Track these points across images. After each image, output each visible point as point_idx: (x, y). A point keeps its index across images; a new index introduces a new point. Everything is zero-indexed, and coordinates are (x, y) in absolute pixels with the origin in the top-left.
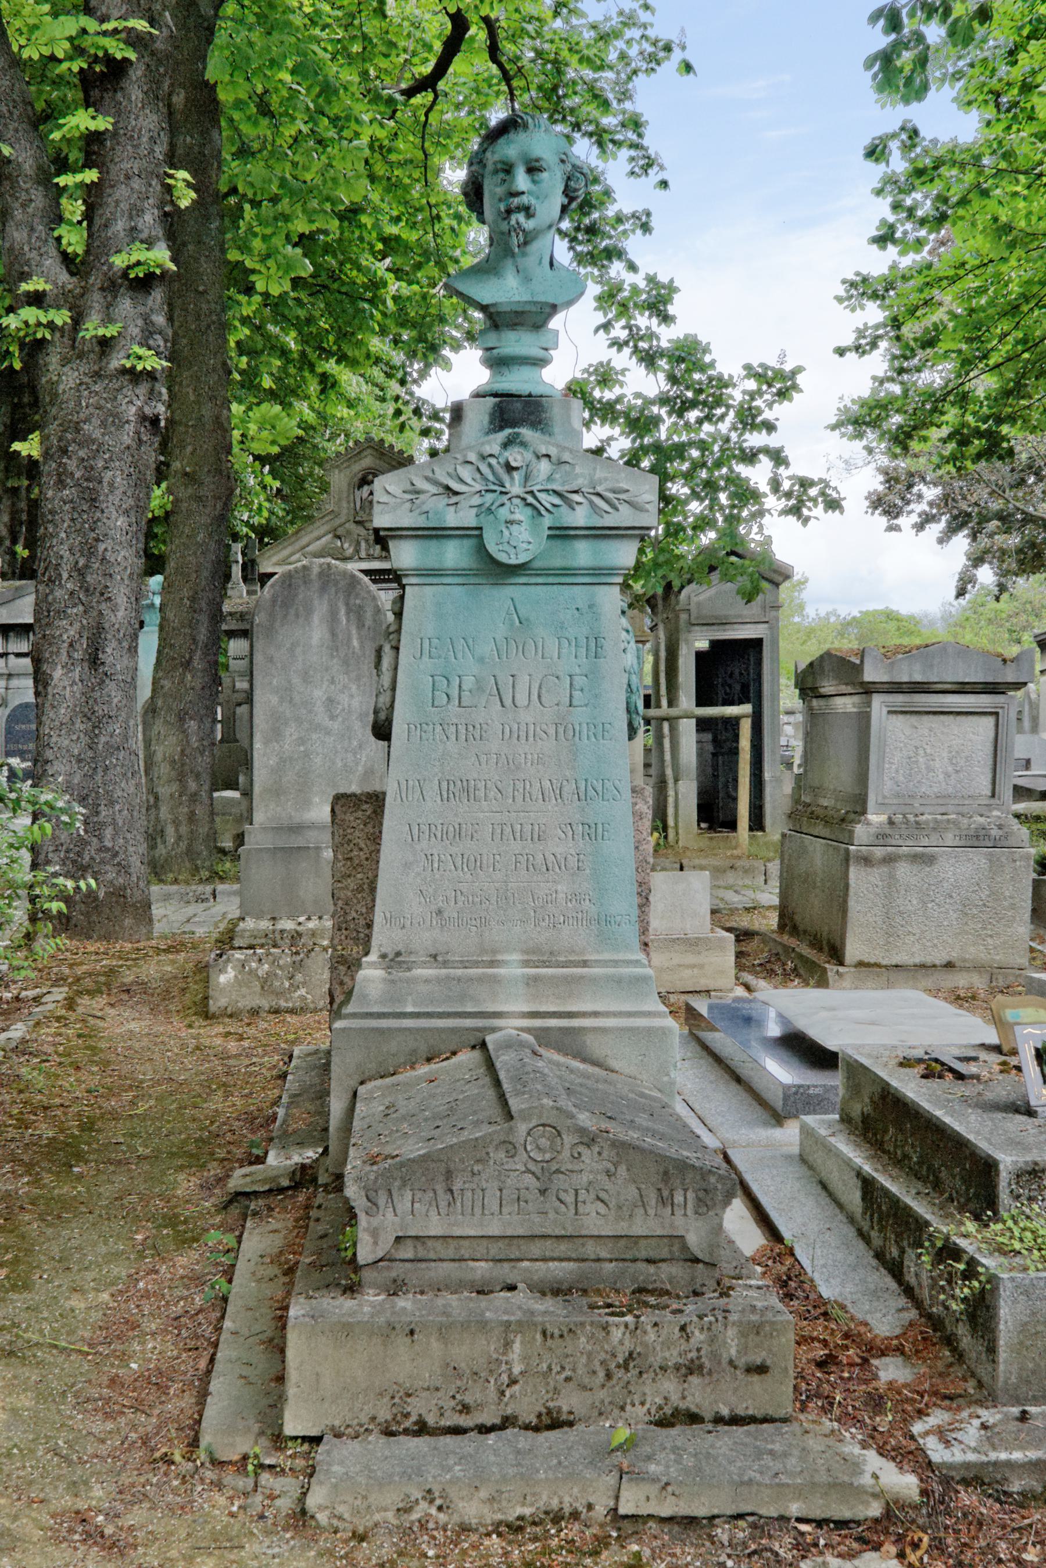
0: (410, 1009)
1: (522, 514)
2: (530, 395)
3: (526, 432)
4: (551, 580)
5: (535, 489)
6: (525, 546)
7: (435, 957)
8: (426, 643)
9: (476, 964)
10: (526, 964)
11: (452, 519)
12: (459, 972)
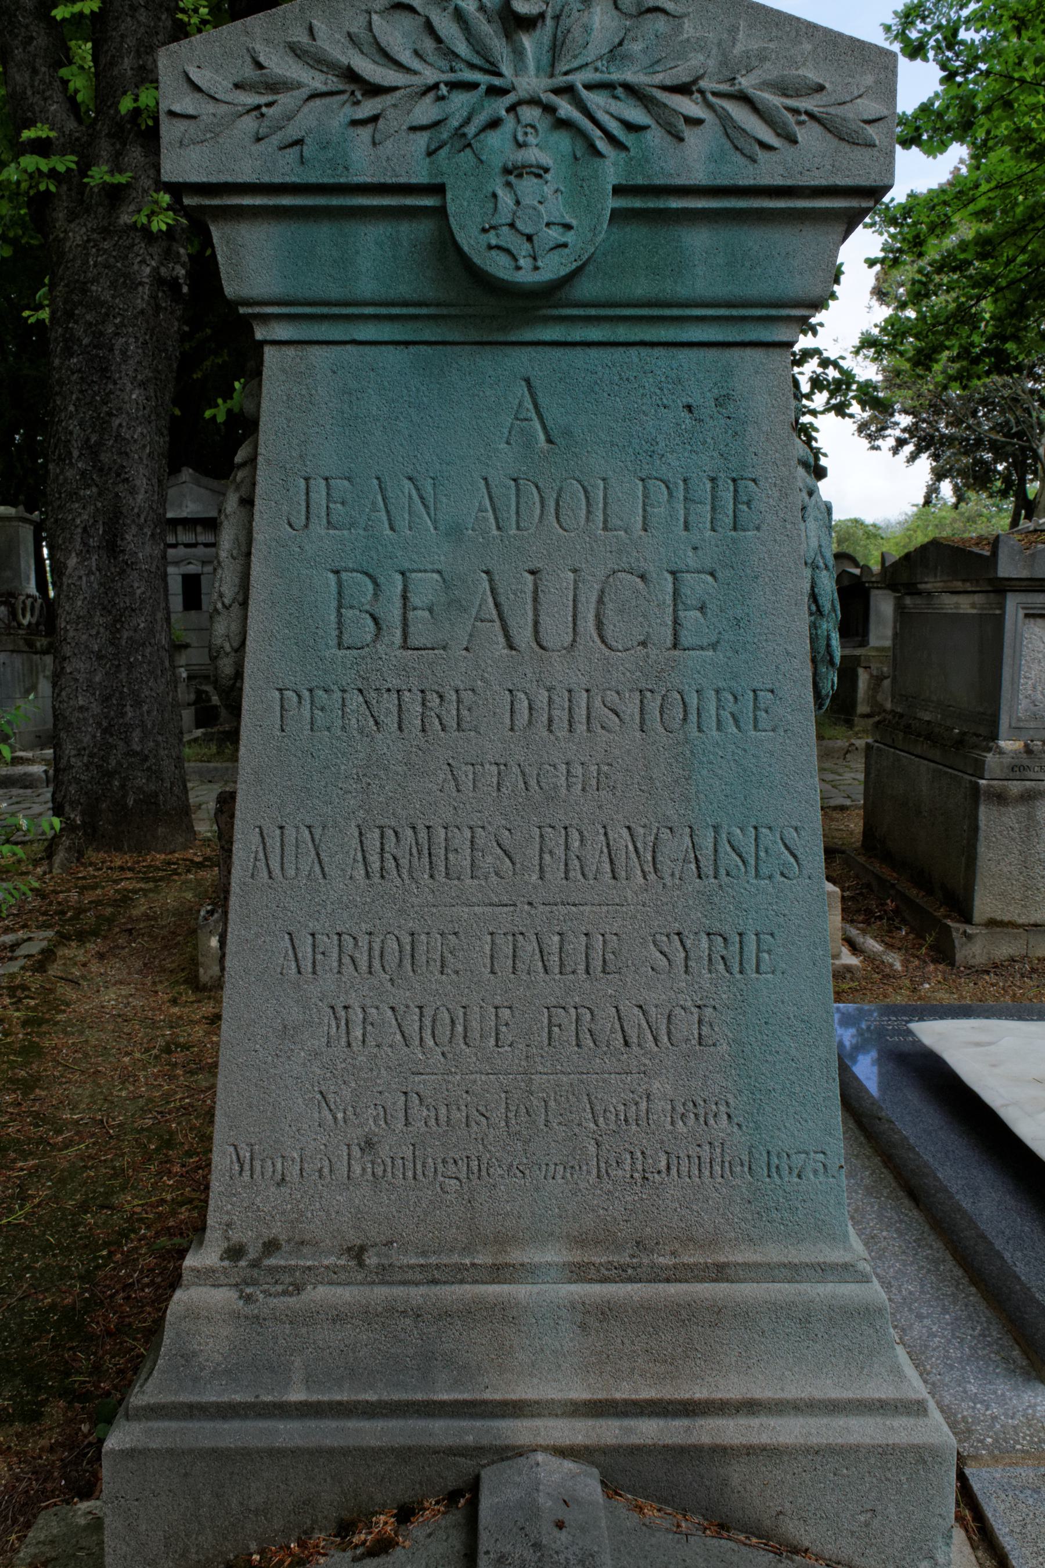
0: (297, 1395)
1: (546, 149)
4: (623, 333)
5: (578, 79)
7: (358, 1253)
8: (319, 494)
9: (459, 1275)
10: (579, 1273)
11: (364, 162)
12: (417, 1294)
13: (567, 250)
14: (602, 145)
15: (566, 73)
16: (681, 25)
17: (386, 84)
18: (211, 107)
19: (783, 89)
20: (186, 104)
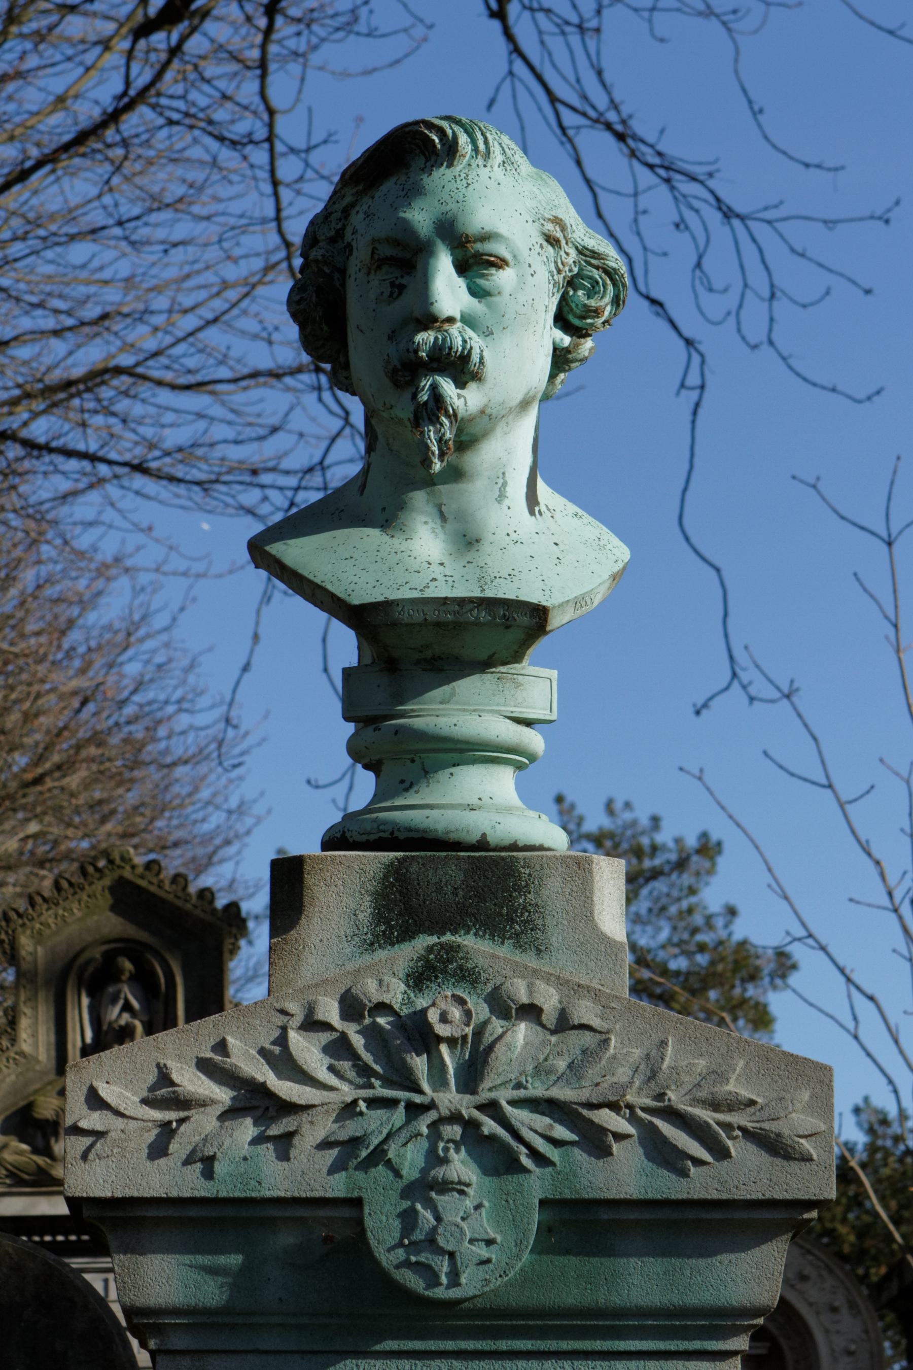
2: (482, 844)
3: (475, 946)
5: (503, 1096)
6: (483, 1252)
13: (491, 1266)
14: (526, 1161)
15: (490, 1090)
16: (606, 1041)
17: (302, 1102)
18: (119, 1123)
19: (715, 1105)
20: (93, 1120)
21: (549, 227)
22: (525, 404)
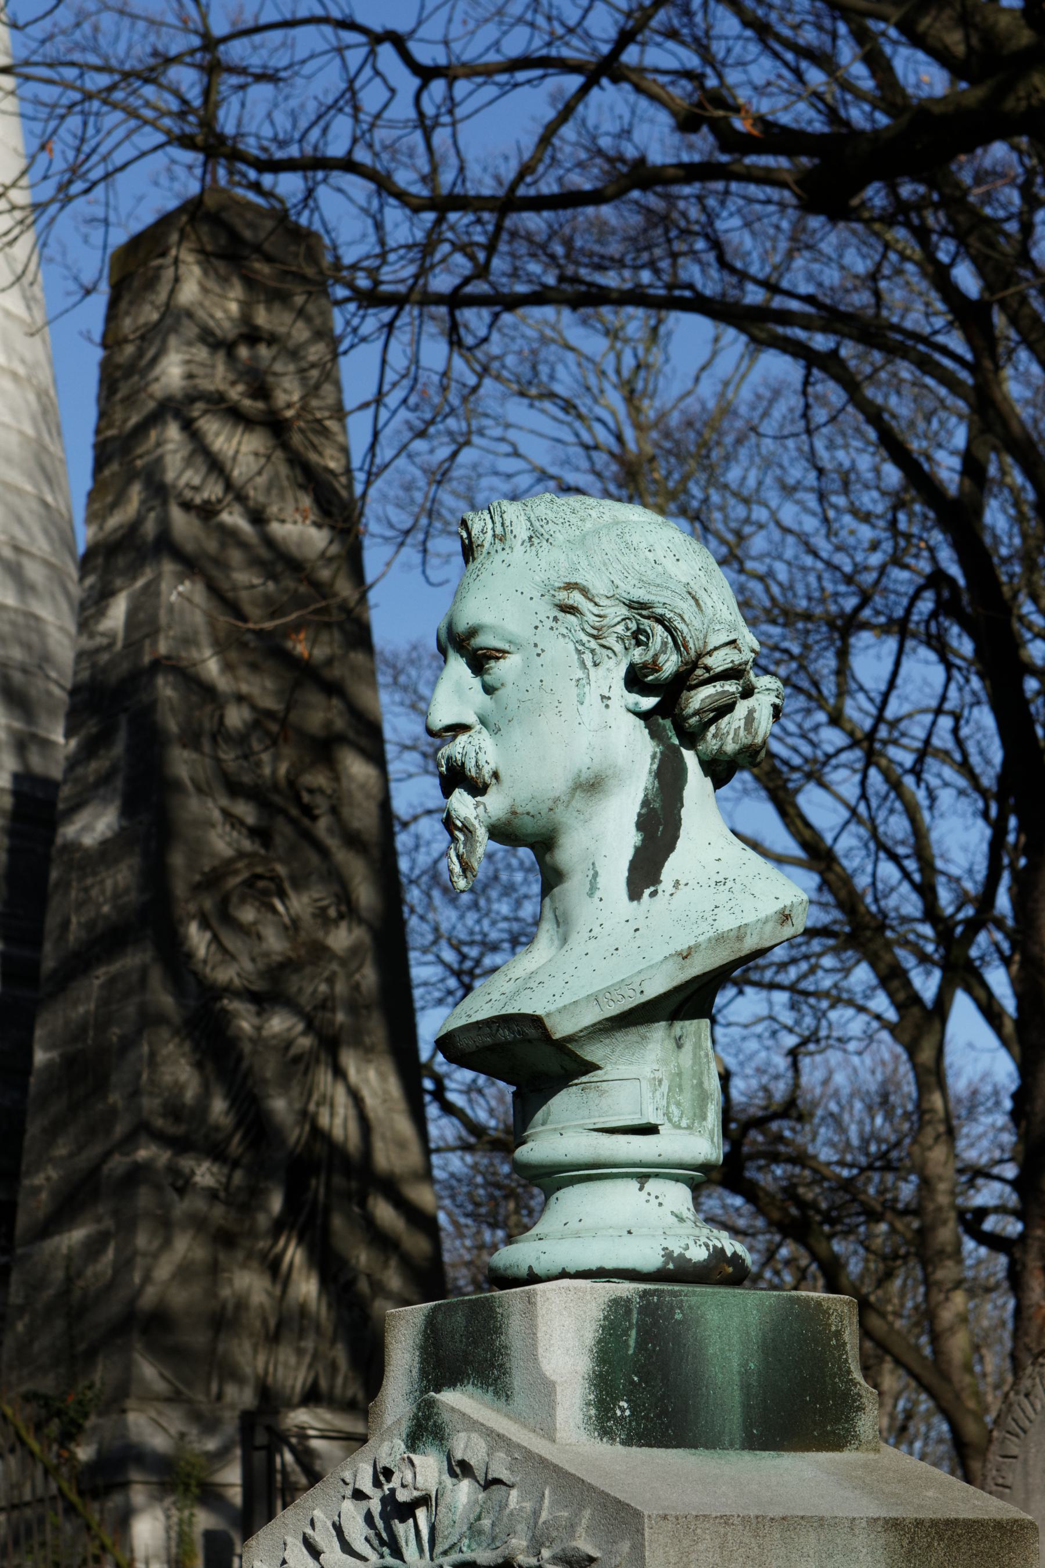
21: (562, 595)
22: (591, 786)
